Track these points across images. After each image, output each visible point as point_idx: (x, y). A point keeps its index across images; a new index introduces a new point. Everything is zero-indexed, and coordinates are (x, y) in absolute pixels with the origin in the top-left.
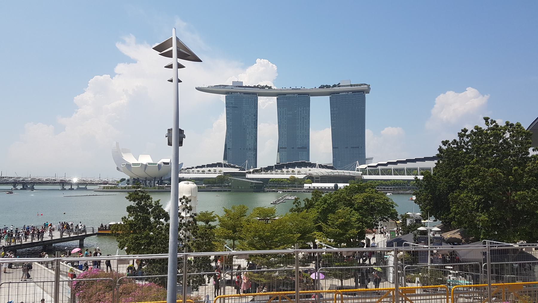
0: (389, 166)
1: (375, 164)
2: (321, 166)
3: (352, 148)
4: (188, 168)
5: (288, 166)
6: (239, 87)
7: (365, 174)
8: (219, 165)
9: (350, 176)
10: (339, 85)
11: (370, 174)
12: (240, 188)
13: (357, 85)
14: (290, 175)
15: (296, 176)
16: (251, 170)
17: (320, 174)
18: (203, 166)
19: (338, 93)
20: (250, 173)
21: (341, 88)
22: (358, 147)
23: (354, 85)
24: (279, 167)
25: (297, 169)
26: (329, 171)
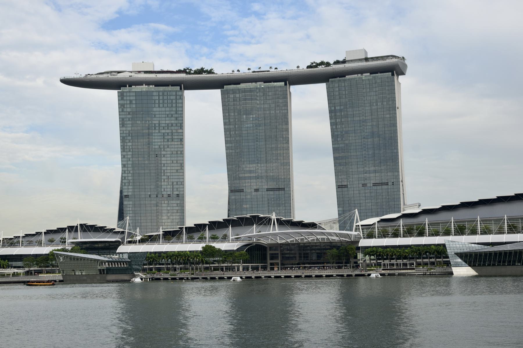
6: (146, 72)
8: (71, 229)
9: (341, 242)
10: (344, 62)
13: (377, 58)
14: (204, 245)
15: (217, 245)
16: (138, 238)
19: (342, 74)
21: (347, 65)
22: (387, 184)
23: (373, 59)
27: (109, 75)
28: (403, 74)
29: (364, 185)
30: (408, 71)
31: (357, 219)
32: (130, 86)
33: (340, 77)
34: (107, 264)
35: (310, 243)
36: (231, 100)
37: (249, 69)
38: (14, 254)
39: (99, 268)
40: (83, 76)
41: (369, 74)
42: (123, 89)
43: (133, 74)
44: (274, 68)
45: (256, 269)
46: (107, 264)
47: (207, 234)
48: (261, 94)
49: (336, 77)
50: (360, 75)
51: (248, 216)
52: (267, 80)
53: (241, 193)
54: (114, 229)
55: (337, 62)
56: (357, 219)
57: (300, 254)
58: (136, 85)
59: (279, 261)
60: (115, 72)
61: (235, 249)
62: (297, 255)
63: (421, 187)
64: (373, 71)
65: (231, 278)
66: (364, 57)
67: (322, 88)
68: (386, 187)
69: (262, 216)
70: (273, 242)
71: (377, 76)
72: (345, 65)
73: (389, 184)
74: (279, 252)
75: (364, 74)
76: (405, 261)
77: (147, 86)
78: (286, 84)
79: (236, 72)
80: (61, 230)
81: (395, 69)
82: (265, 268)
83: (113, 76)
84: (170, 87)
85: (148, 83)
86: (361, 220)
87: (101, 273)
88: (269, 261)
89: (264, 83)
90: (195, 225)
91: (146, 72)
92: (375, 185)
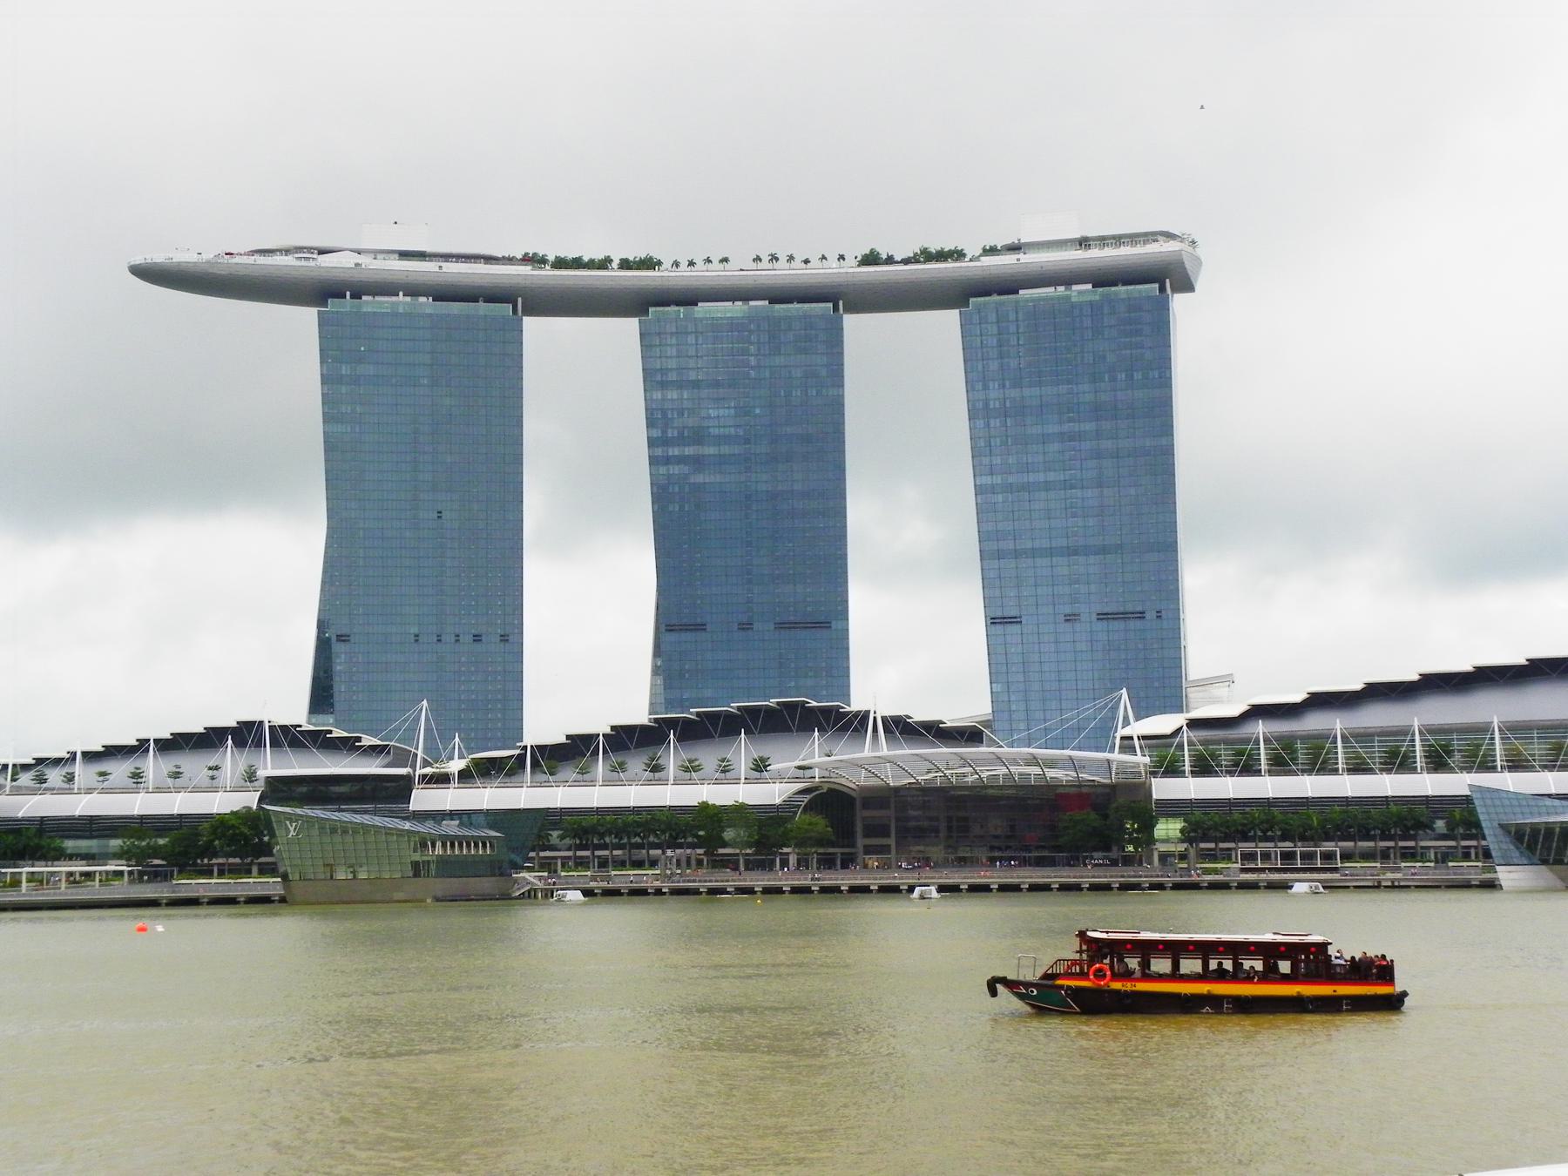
0: (1314, 722)
1: (1234, 711)
2: (901, 728)
3: (1103, 616)
4: (40, 761)
5: (695, 731)
6: (405, 255)
7: (1173, 770)
8: (246, 734)
9: (1080, 784)
11: (1204, 768)
12: (341, 875)
13: (1118, 240)
16: (456, 766)
17: (892, 778)
18: (141, 747)
19: (1007, 286)
20: (442, 779)
22: (1141, 615)
23: (1103, 241)
24: (624, 739)
25: (743, 751)
26: (943, 751)
29: (1070, 618)
30: (1199, 285)
31: (1126, 719)
32: (356, 295)
33: (1000, 294)
34: (439, 844)
35: (986, 787)
36: (672, 351)
37: (725, 260)
38: (77, 813)
39: (417, 857)
40: (208, 256)
41: (1089, 286)
42: (333, 305)
43: (365, 261)
44: (799, 258)
45: (827, 863)
46: (439, 844)
47: (672, 757)
48: (765, 338)
49: (988, 294)
50: (1061, 289)
51: (772, 702)
52: (779, 296)
53: (701, 636)
54: (359, 739)
55: (991, 251)
56: (1126, 719)
57: (949, 819)
58: (374, 295)
59: (892, 841)
60: (310, 249)
61: (778, 801)
62: (943, 826)
63: (1259, 629)
64: (1103, 278)
65: (911, 889)
66: (1078, 236)
67: (947, 322)
68: (1138, 623)
69: (814, 704)
70: (873, 782)
71: (1116, 293)
72: (1021, 256)
73: (1148, 616)
74: (891, 812)
75: (1075, 287)
76: (1287, 846)
77: (408, 299)
78: (836, 308)
80: (210, 739)
81: (1171, 277)
82: (847, 862)
83: (303, 263)
84: (481, 303)
85: (413, 290)
86: (1138, 718)
87: (417, 874)
88: (861, 842)
89: (774, 300)
90: (613, 728)
91: (405, 255)
92: (1103, 616)
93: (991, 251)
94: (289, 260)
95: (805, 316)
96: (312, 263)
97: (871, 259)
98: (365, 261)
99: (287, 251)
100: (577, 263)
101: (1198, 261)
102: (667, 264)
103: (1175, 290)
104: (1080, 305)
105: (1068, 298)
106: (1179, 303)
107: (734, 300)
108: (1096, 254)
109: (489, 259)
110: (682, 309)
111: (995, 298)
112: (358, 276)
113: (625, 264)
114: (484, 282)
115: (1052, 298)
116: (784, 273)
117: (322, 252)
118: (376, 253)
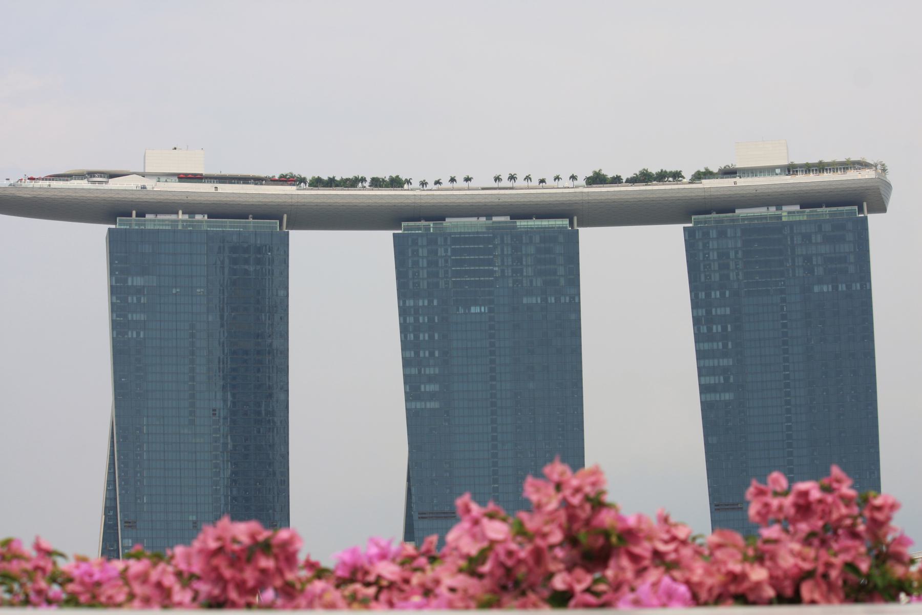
13: (821, 167)
19: (725, 205)
21: (742, 182)
23: (808, 168)
27: (85, 181)
28: (883, 209)
32: (141, 214)
33: (719, 211)
42: (120, 224)
43: (150, 184)
49: (709, 212)
50: (773, 209)
58: (156, 213)
60: (102, 174)
72: (737, 179)
75: (786, 208)
77: (186, 217)
78: (571, 224)
79: (431, 185)
83: (97, 186)
85: (191, 208)
93: (708, 174)
94: (83, 184)
95: (544, 229)
96: (104, 186)
97: (597, 179)
98: (150, 184)
99: (80, 176)
100: (331, 183)
101: (888, 186)
102: (416, 183)
103: (872, 210)
104: (791, 224)
105: (780, 217)
106: (874, 220)
107: (478, 216)
108: (801, 179)
109: (258, 180)
110: (431, 224)
111: (714, 215)
112: (143, 196)
113: (376, 183)
114: (251, 200)
115: (765, 218)
116: (523, 192)
117: (112, 176)
118: (159, 176)
